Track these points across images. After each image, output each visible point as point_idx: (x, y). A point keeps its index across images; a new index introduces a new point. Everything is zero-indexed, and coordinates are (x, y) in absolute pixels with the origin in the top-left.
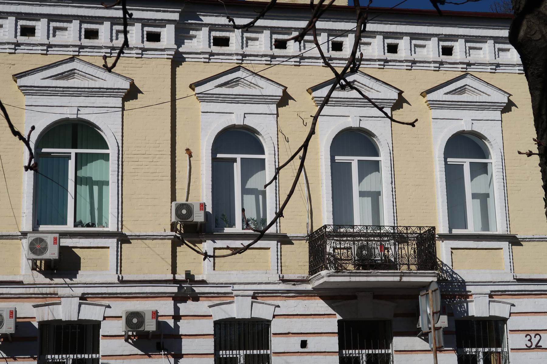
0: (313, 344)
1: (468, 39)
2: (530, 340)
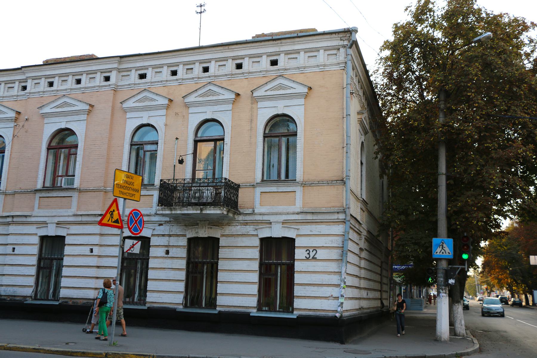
0: (173, 252)
1: (287, 53)
2: (309, 254)
